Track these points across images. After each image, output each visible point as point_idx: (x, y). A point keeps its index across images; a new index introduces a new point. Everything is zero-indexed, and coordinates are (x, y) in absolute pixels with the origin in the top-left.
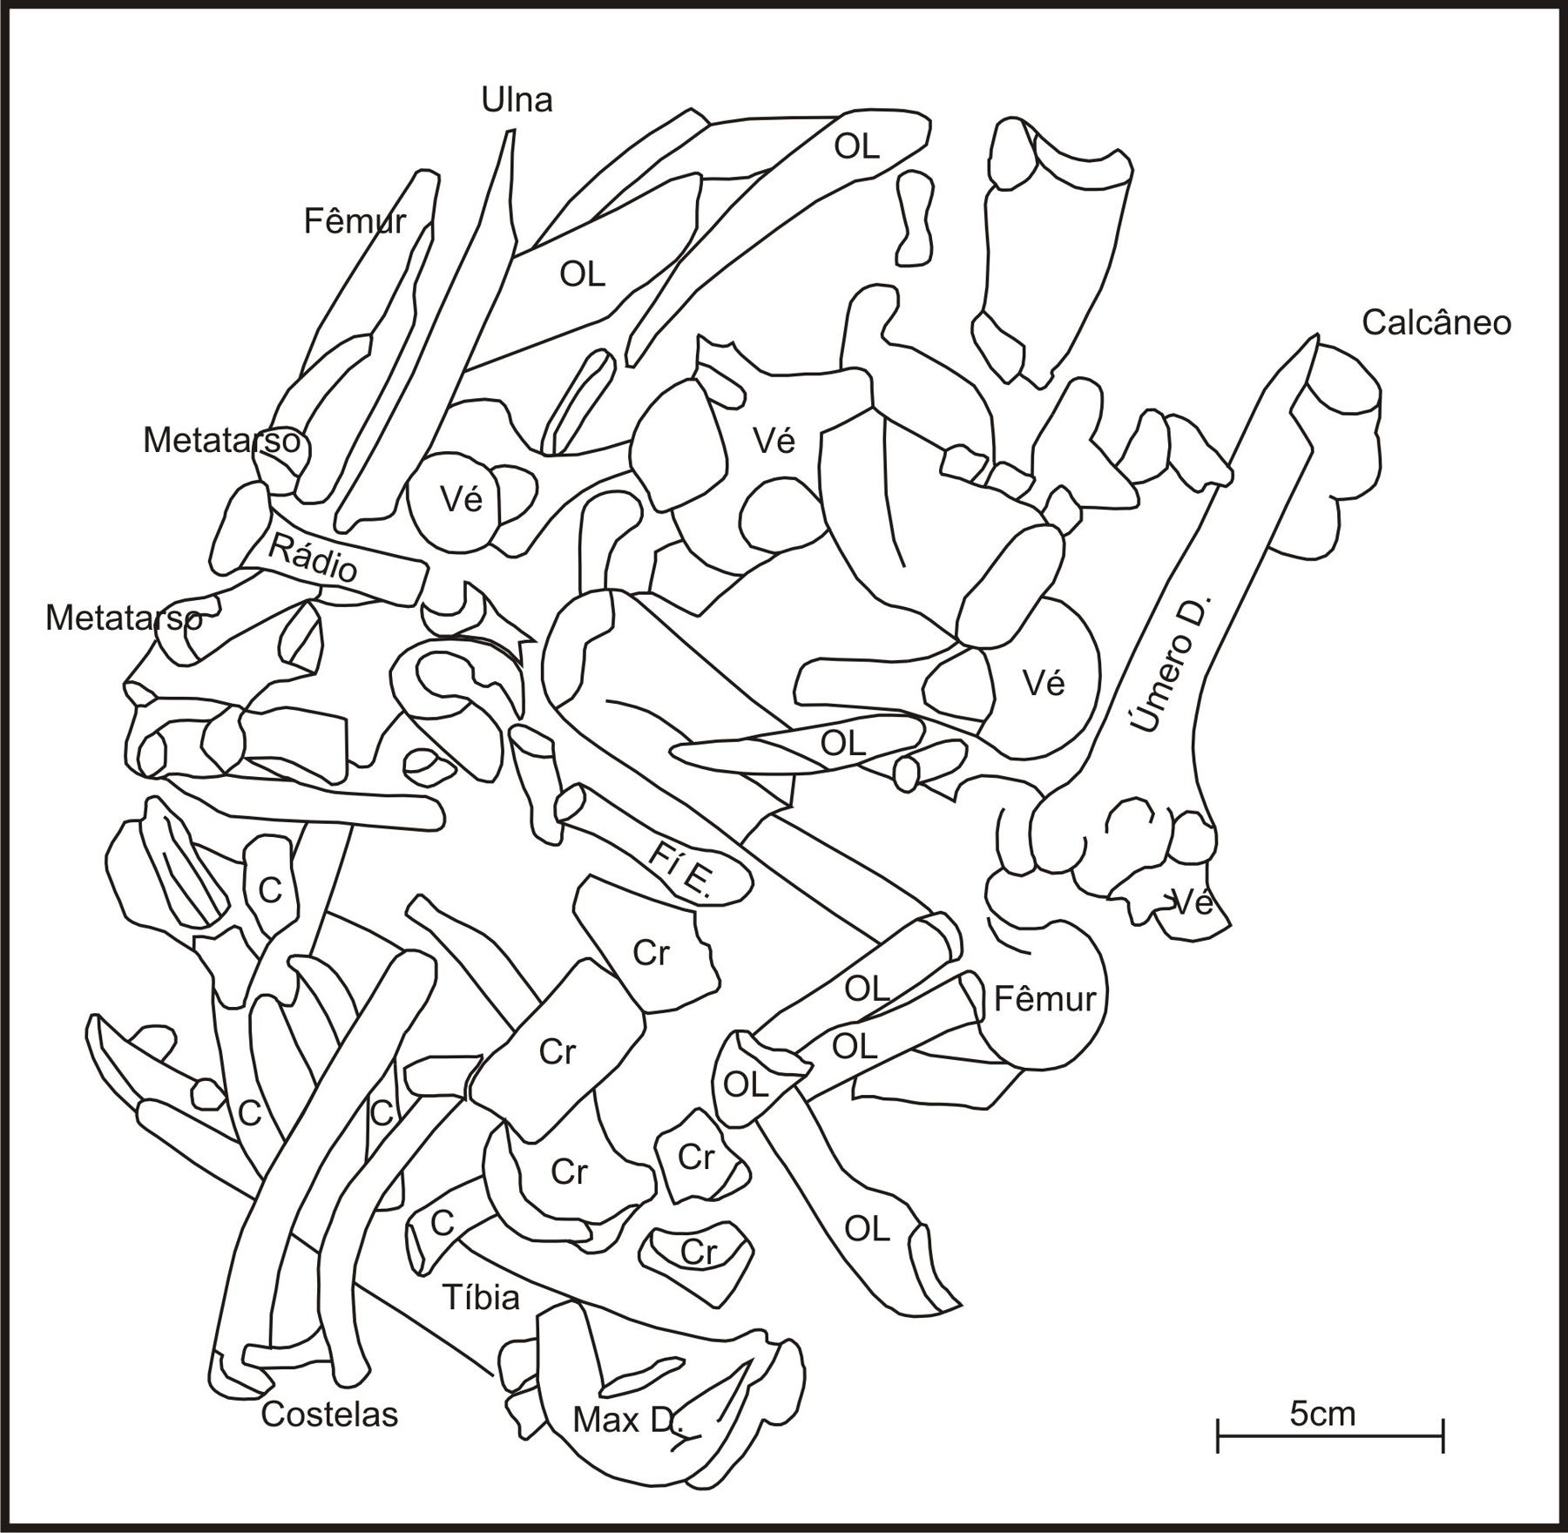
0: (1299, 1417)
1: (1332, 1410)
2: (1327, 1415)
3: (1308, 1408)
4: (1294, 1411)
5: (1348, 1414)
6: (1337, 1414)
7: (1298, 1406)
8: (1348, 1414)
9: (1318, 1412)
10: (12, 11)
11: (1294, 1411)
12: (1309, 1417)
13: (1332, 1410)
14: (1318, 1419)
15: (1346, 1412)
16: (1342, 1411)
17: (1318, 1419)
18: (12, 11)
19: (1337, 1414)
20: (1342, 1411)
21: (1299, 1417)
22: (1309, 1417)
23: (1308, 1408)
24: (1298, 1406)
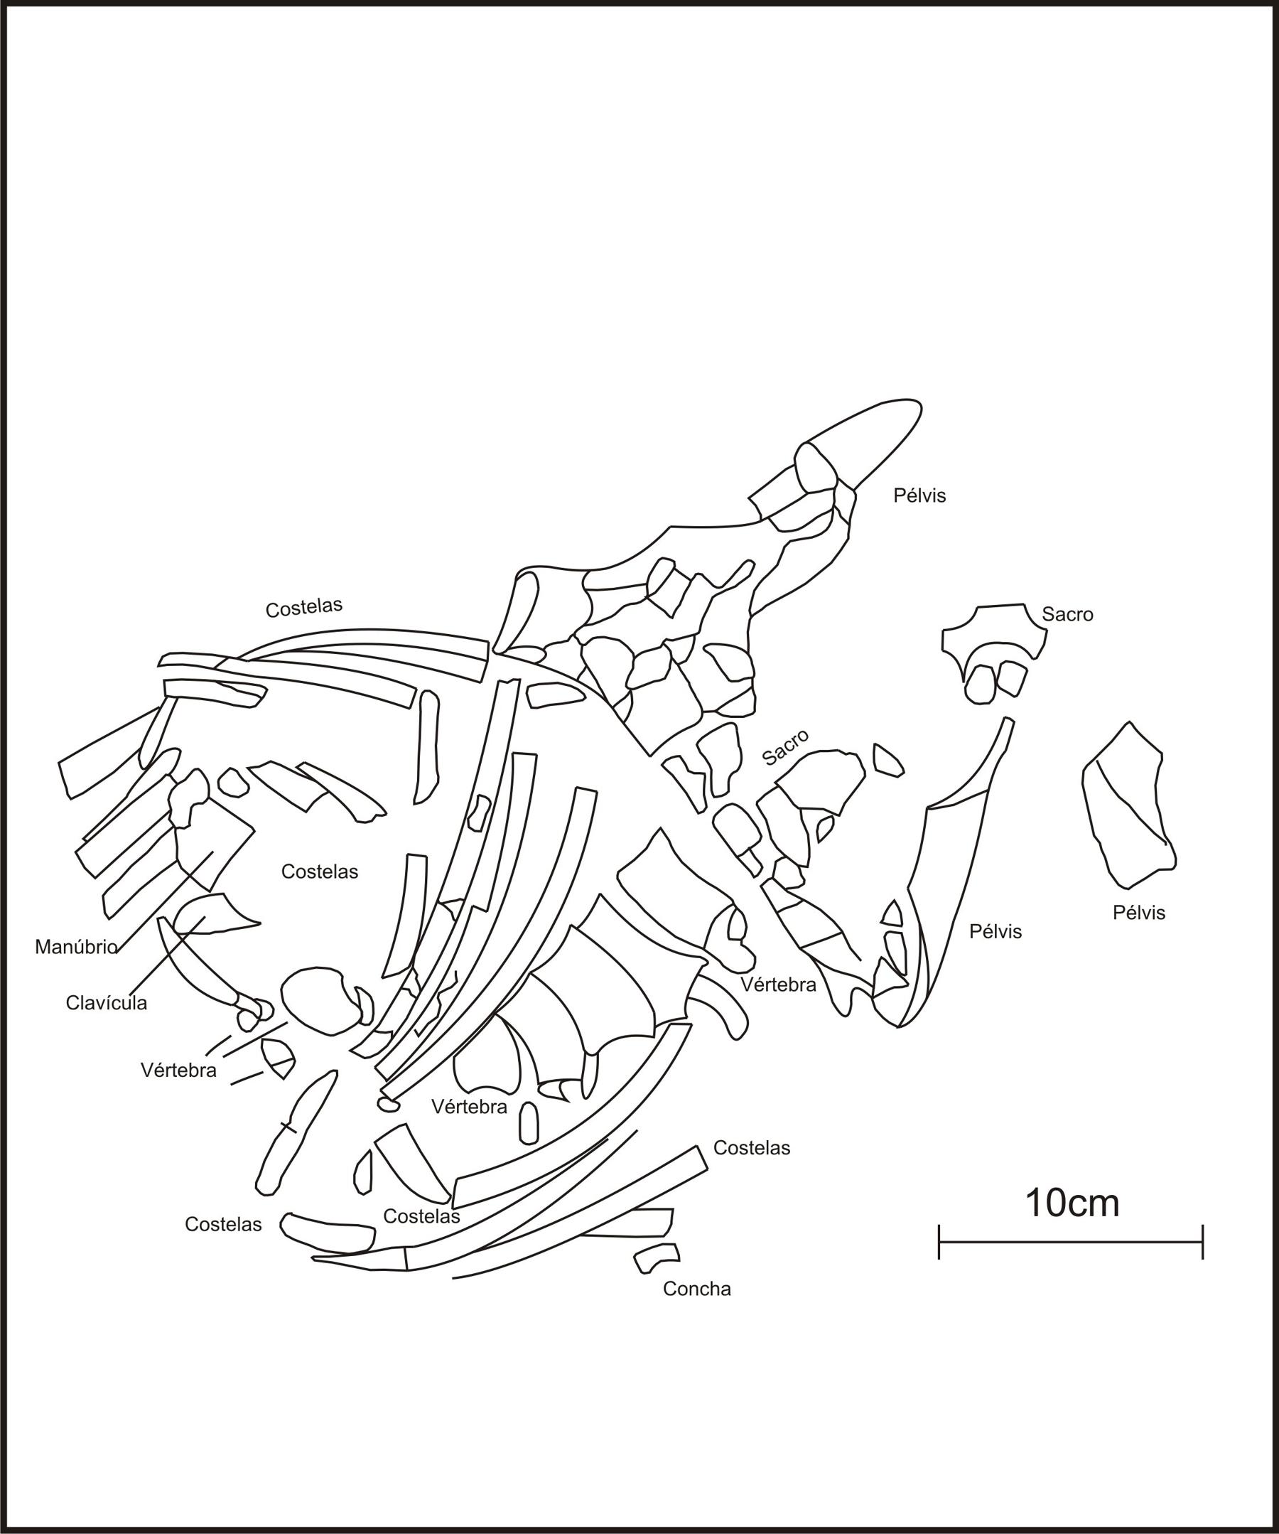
1: (1092, 1199)
2: (1087, 1205)
5: (1110, 1203)
6: (1098, 1202)
8: (1110, 1203)
9: (1077, 1202)
10: (11, 10)
12: (1067, 1204)
13: (1092, 1199)
14: (1078, 1210)
15: (1107, 1202)
16: (1104, 1200)
17: (1078, 1210)
18: (11, 10)
19: (1098, 1202)
20: (1104, 1200)
22: (1067, 1204)
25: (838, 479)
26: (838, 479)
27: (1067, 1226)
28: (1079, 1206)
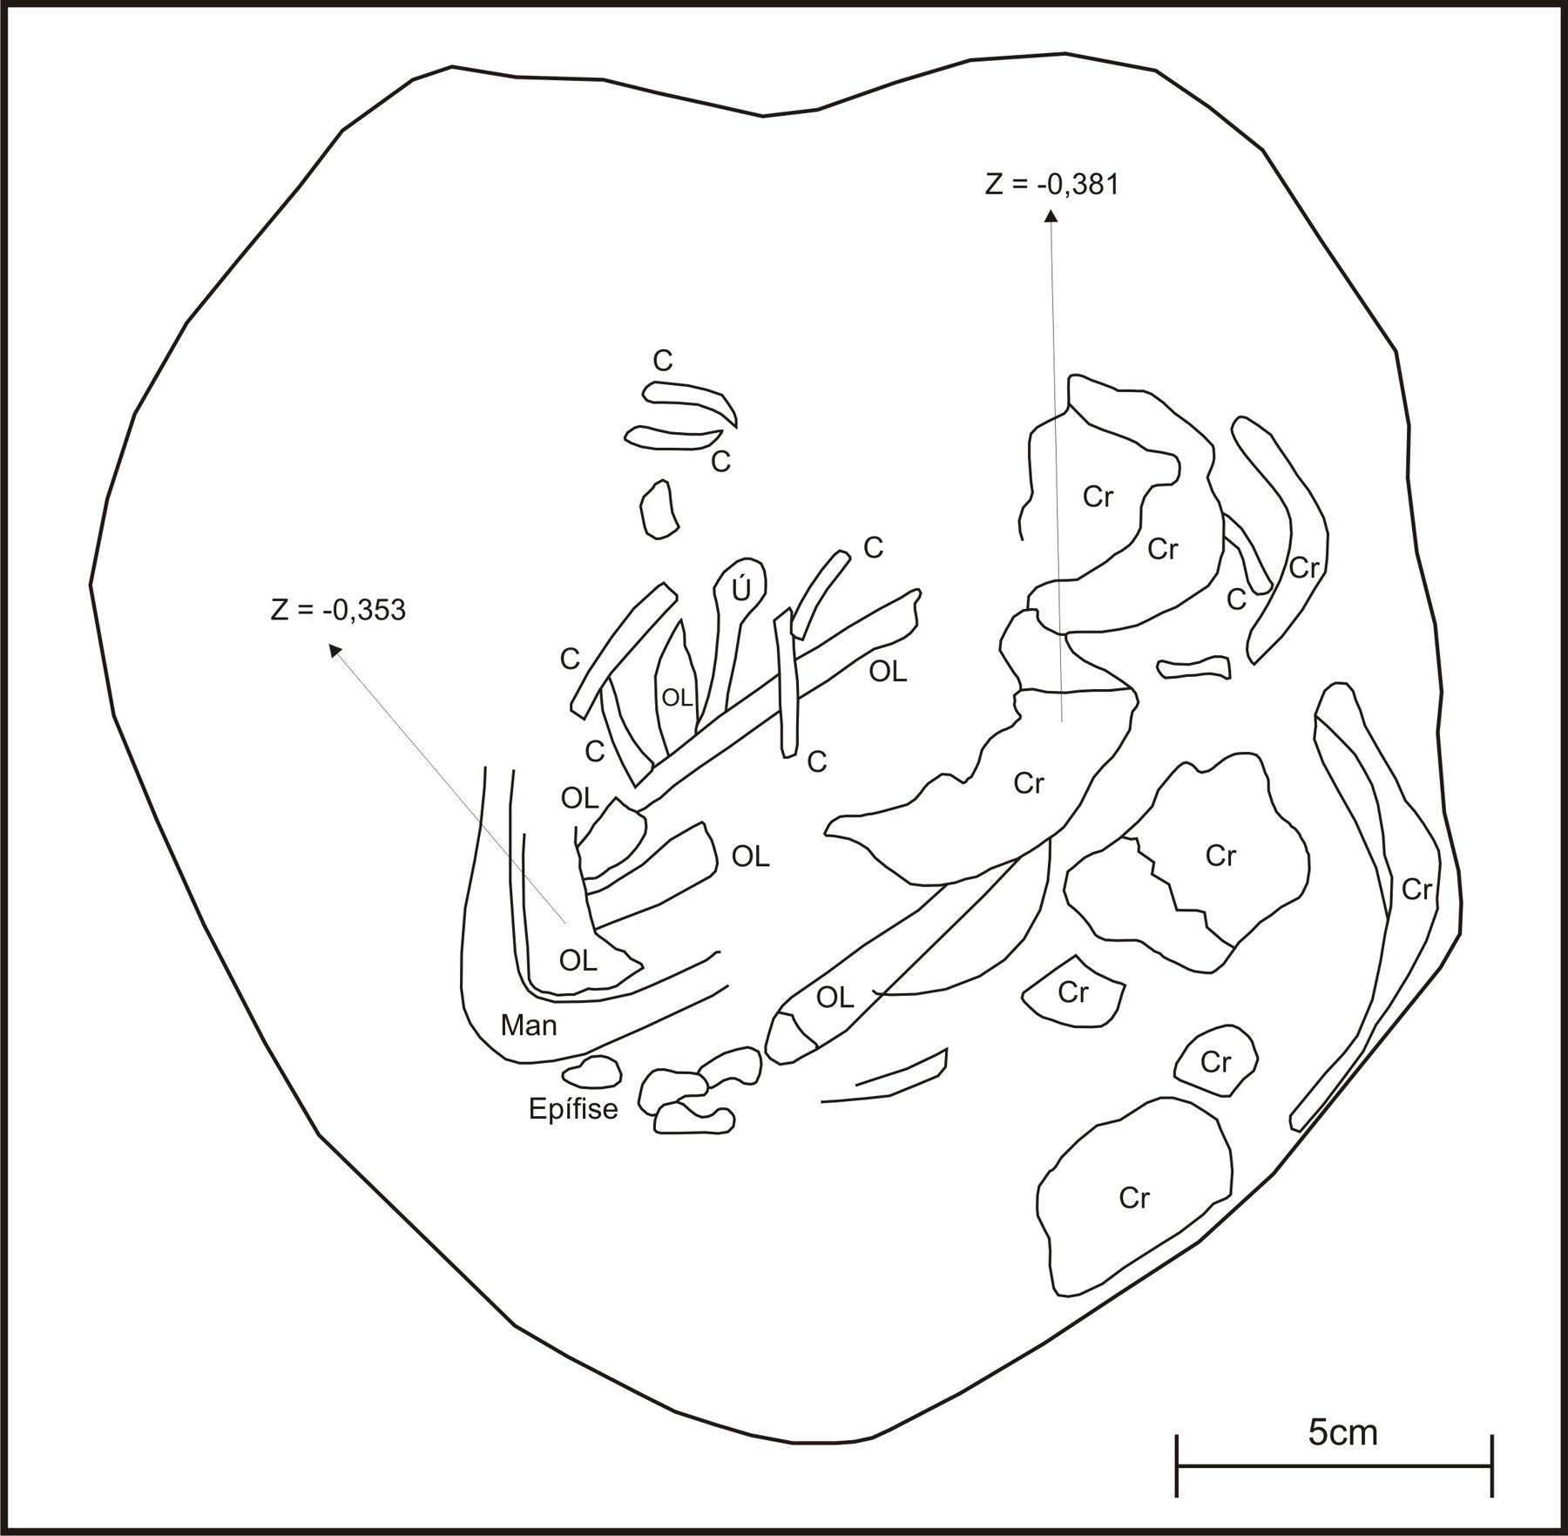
0: (1318, 1436)
1: (1352, 1429)
2: (1347, 1434)
3: (1328, 1427)
4: (1312, 1430)
5: (1369, 1432)
6: (1358, 1432)
7: (1317, 1424)
8: (1369, 1432)
11: (1312, 1430)
13: (1352, 1429)
14: (1338, 1439)
15: (1366, 1432)
16: (1363, 1430)
17: (1338, 1439)
19: (1358, 1432)
20: (1363, 1430)
21: (1318, 1436)
22: (1329, 1436)
23: (1328, 1427)
24: (1317, 1424)
25: (1069, 405)
26: (1069, 405)
27: (1329, 1453)
28: (1340, 1435)
